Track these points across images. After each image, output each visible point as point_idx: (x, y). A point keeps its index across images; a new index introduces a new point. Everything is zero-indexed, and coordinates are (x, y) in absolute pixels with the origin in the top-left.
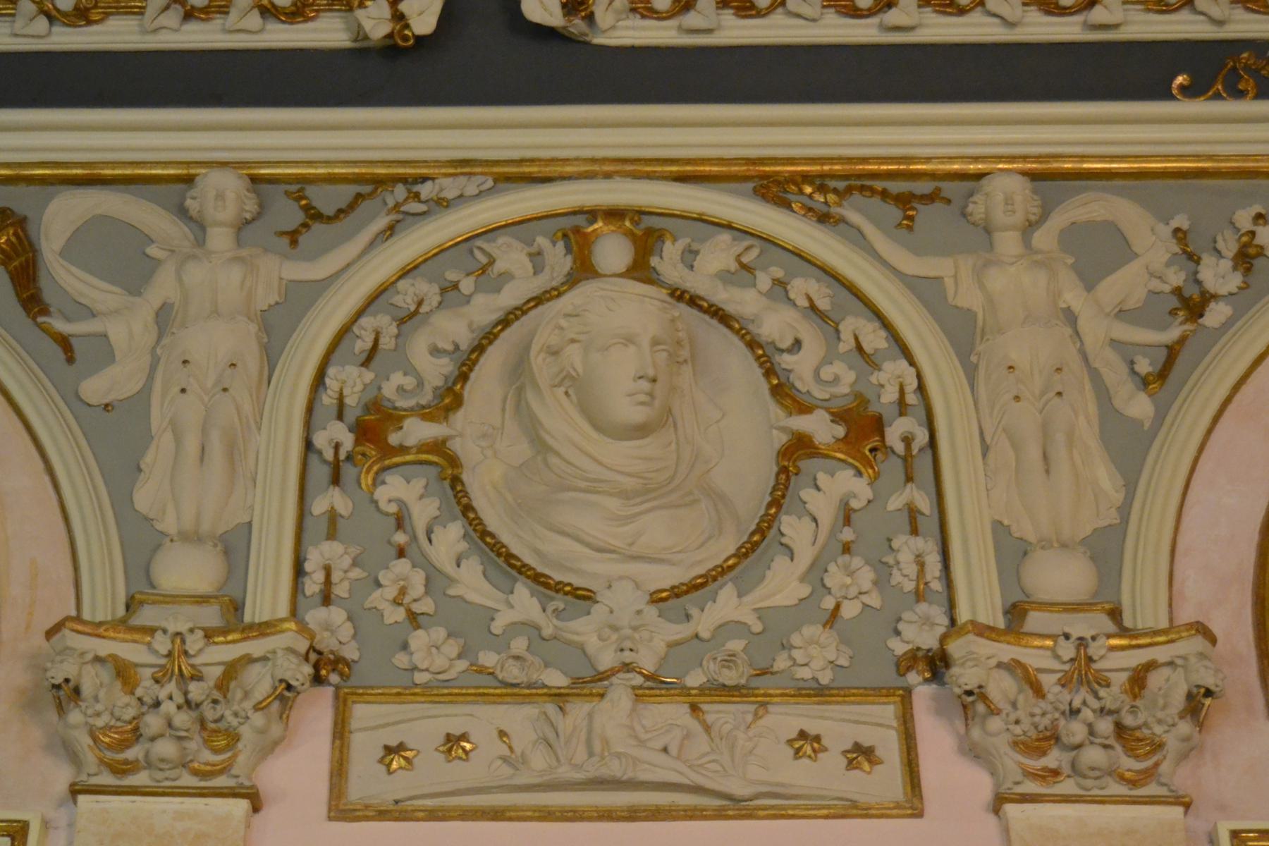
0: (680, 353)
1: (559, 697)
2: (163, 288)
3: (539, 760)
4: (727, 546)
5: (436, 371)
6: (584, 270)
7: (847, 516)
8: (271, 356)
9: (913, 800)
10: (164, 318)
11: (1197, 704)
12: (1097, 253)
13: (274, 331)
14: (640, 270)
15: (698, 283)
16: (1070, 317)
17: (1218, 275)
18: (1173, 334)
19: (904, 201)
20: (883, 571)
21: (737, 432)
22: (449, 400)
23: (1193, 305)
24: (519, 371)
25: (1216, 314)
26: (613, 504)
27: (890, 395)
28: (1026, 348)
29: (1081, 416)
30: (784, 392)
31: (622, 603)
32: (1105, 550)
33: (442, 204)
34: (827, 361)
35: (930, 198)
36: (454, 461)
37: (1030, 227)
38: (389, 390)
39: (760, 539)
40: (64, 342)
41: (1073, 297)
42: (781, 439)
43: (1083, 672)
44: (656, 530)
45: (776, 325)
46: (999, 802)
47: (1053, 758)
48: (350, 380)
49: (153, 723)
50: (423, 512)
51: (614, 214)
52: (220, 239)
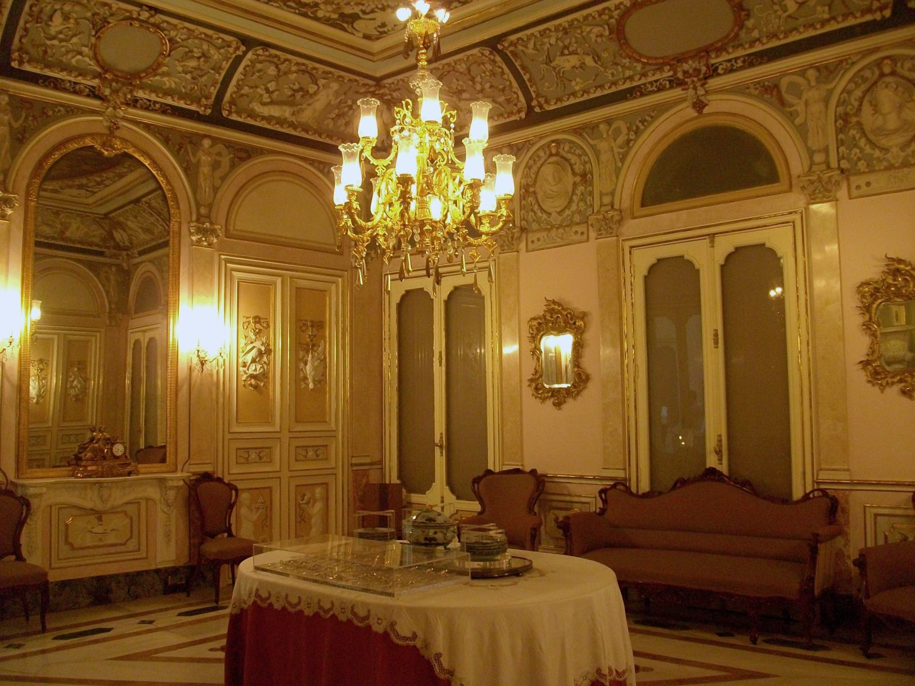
4: (566, 203)
17: (632, 137)
23: (629, 141)
28: (604, 157)
31: (554, 214)
32: (612, 194)
39: (571, 201)
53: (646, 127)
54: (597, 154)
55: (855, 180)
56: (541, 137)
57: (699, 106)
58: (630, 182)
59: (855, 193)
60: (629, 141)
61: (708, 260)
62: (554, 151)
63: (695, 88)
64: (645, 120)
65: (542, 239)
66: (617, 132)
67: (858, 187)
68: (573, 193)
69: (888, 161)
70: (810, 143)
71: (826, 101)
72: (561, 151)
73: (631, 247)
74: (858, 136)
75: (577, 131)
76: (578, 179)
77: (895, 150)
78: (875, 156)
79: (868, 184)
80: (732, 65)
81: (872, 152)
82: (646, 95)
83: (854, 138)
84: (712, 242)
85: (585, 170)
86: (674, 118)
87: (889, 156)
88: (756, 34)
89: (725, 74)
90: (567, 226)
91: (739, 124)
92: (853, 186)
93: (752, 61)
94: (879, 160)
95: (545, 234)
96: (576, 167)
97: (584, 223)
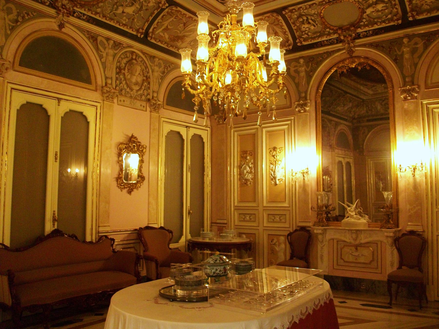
11: (7, 69)
16: (5, 19)
17: (20, 19)
18: (14, 25)
23: (17, 21)
25: (19, 23)
37: (4, 6)
41: (6, 17)
57: (61, 26)
58: (13, 47)
59: (119, 102)
61: (56, 112)
63: (63, 16)
67: (120, 101)
69: (131, 94)
73: (12, 88)
77: (134, 91)
79: (124, 101)
80: (81, 16)
83: (121, 79)
84: (59, 102)
87: (132, 92)
88: (99, 10)
89: (76, 17)
93: (90, 20)
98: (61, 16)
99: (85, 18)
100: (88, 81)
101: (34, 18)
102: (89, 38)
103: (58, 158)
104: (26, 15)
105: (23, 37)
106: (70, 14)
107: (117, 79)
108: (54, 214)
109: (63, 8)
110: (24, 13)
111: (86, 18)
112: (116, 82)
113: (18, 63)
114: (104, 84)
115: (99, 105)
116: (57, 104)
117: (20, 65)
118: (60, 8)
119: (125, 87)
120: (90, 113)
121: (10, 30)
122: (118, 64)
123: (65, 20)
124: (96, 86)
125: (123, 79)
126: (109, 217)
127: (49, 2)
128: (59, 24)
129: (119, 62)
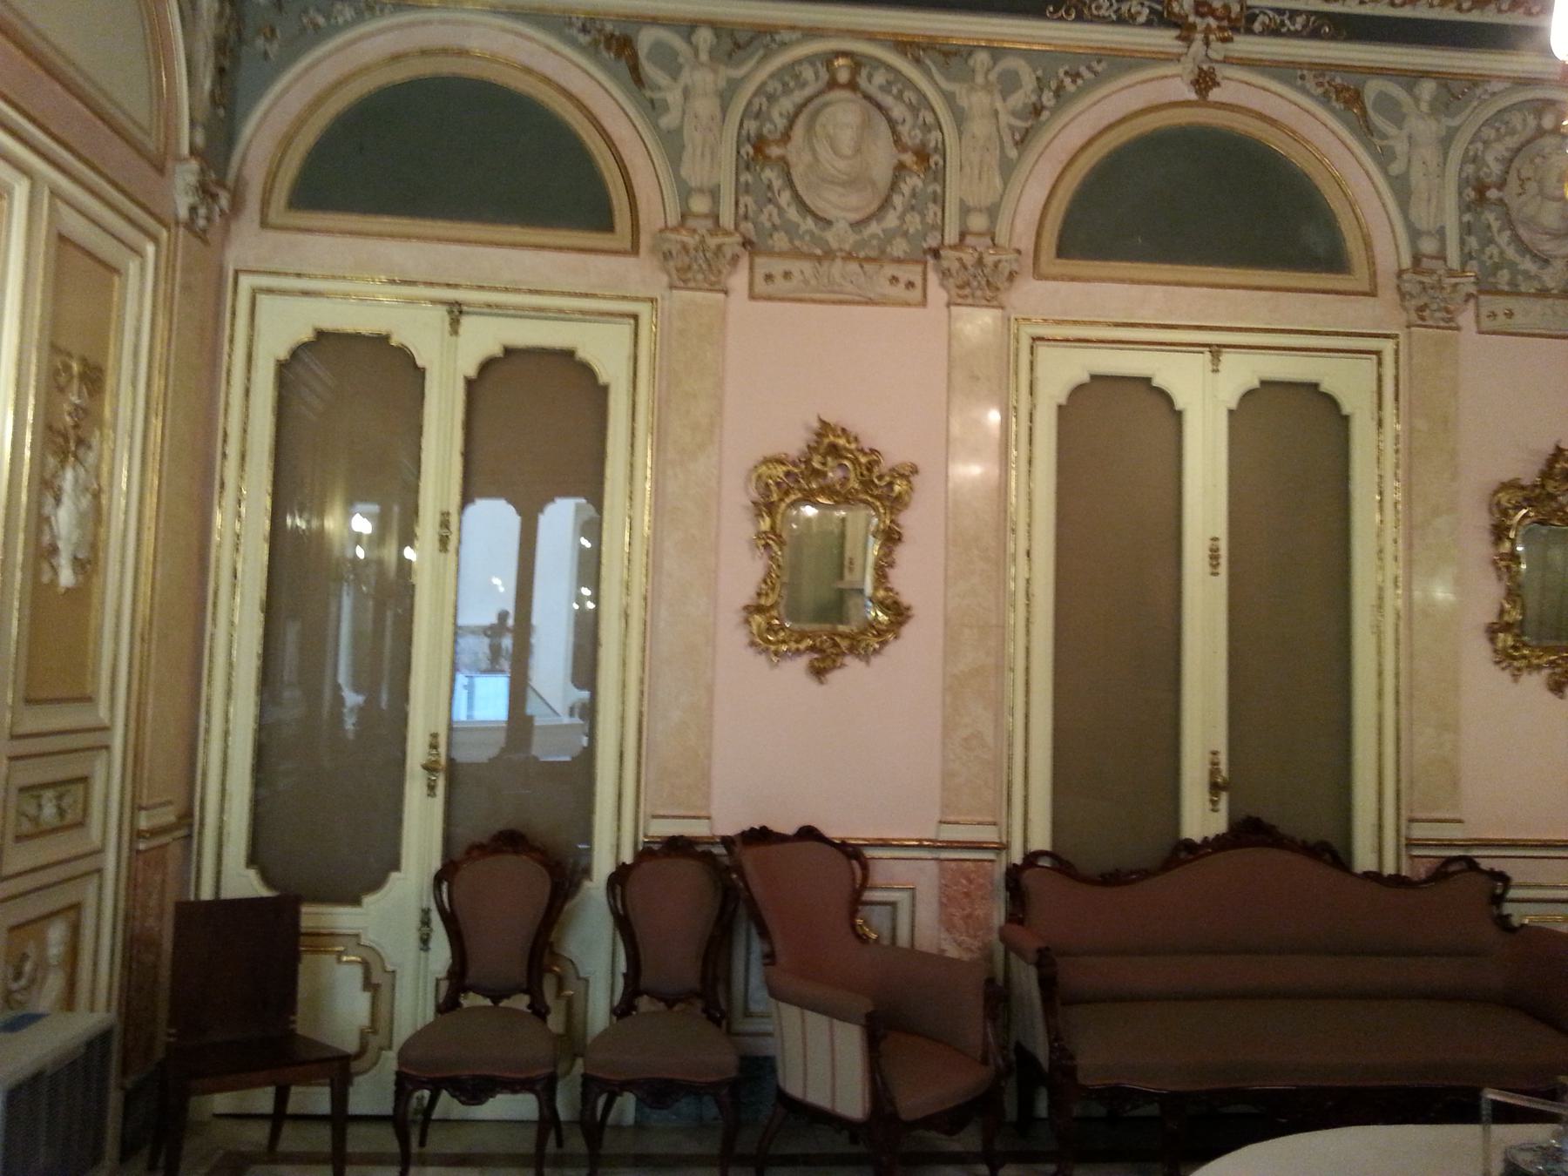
0: (866, 124)
1: (819, 259)
2: (686, 77)
3: (813, 282)
4: (874, 206)
5: (781, 123)
6: (833, 84)
7: (914, 194)
8: (724, 111)
9: (923, 303)
10: (687, 93)
11: (1011, 276)
12: (1009, 83)
13: (725, 97)
14: (852, 85)
15: (872, 90)
16: (996, 113)
17: (1048, 99)
18: (1029, 124)
19: (946, 54)
20: (923, 216)
21: (882, 157)
22: (786, 137)
23: (1037, 110)
24: (810, 128)
25: (1045, 115)
26: (840, 190)
27: (932, 144)
28: (979, 128)
29: (993, 159)
30: (897, 141)
31: (841, 226)
32: (993, 212)
33: (784, 45)
34: (913, 127)
35: (956, 54)
36: (787, 164)
37: (989, 71)
38: (765, 131)
39: (886, 204)
40: (652, 102)
41: (999, 105)
42: (895, 161)
43: (980, 262)
44: (853, 200)
45: (898, 111)
46: (949, 305)
47: (967, 291)
48: (752, 126)
49: (695, 267)
50: (777, 184)
51: (845, 54)
52: (704, 57)
53: (1081, 92)
54: (960, 117)
55: (764, 264)
56: (812, 33)
57: (1204, 81)
58: (1033, 197)
60: (1037, 110)
61: (1205, 396)
62: (843, 76)
63: (1207, 43)
64: (1078, 75)
65: (796, 273)
66: (1009, 83)
67: (1493, 315)
68: (894, 186)
70: (1414, 213)
71: (1446, 142)
72: (862, 81)
73: (1035, 339)
74: (1495, 225)
75: (904, 45)
76: (775, 151)
78: (1522, 267)
79: (1510, 314)
80: (1283, 24)
81: (1518, 259)
82: (1091, 21)
85: (924, 144)
86: (1145, 87)
89: (1262, 34)
90: (868, 259)
91: (1278, 143)
92: (1484, 312)
94: (1527, 276)
95: (807, 266)
96: (904, 130)
97: (917, 262)
98: (1198, 45)
99: (1298, 27)
100: (1333, 260)
101: (1100, 79)
102: (1324, 100)
103: (1224, 561)
104: (1068, 81)
105: (1065, 158)
106: (1236, 30)
107: (1467, 229)
108: (1215, 764)
109: (1202, 15)
110: (1061, 74)
111: (1304, 27)
112: (1462, 242)
113: (1053, 250)
114: (1407, 262)
115: (1387, 346)
116: (1210, 367)
117: (1062, 252)
118: (1192, 19)
119: (1511, 253)
120: (1348, 382)
121: (1016, 144)
122: (1470, 169)
123: (1213, 55)
124: (1373, 275)
125: (1495, 225)
126: (1455, 784)
127: (1146, 11)
128: (1192, 77)
129: (1475, 160)
